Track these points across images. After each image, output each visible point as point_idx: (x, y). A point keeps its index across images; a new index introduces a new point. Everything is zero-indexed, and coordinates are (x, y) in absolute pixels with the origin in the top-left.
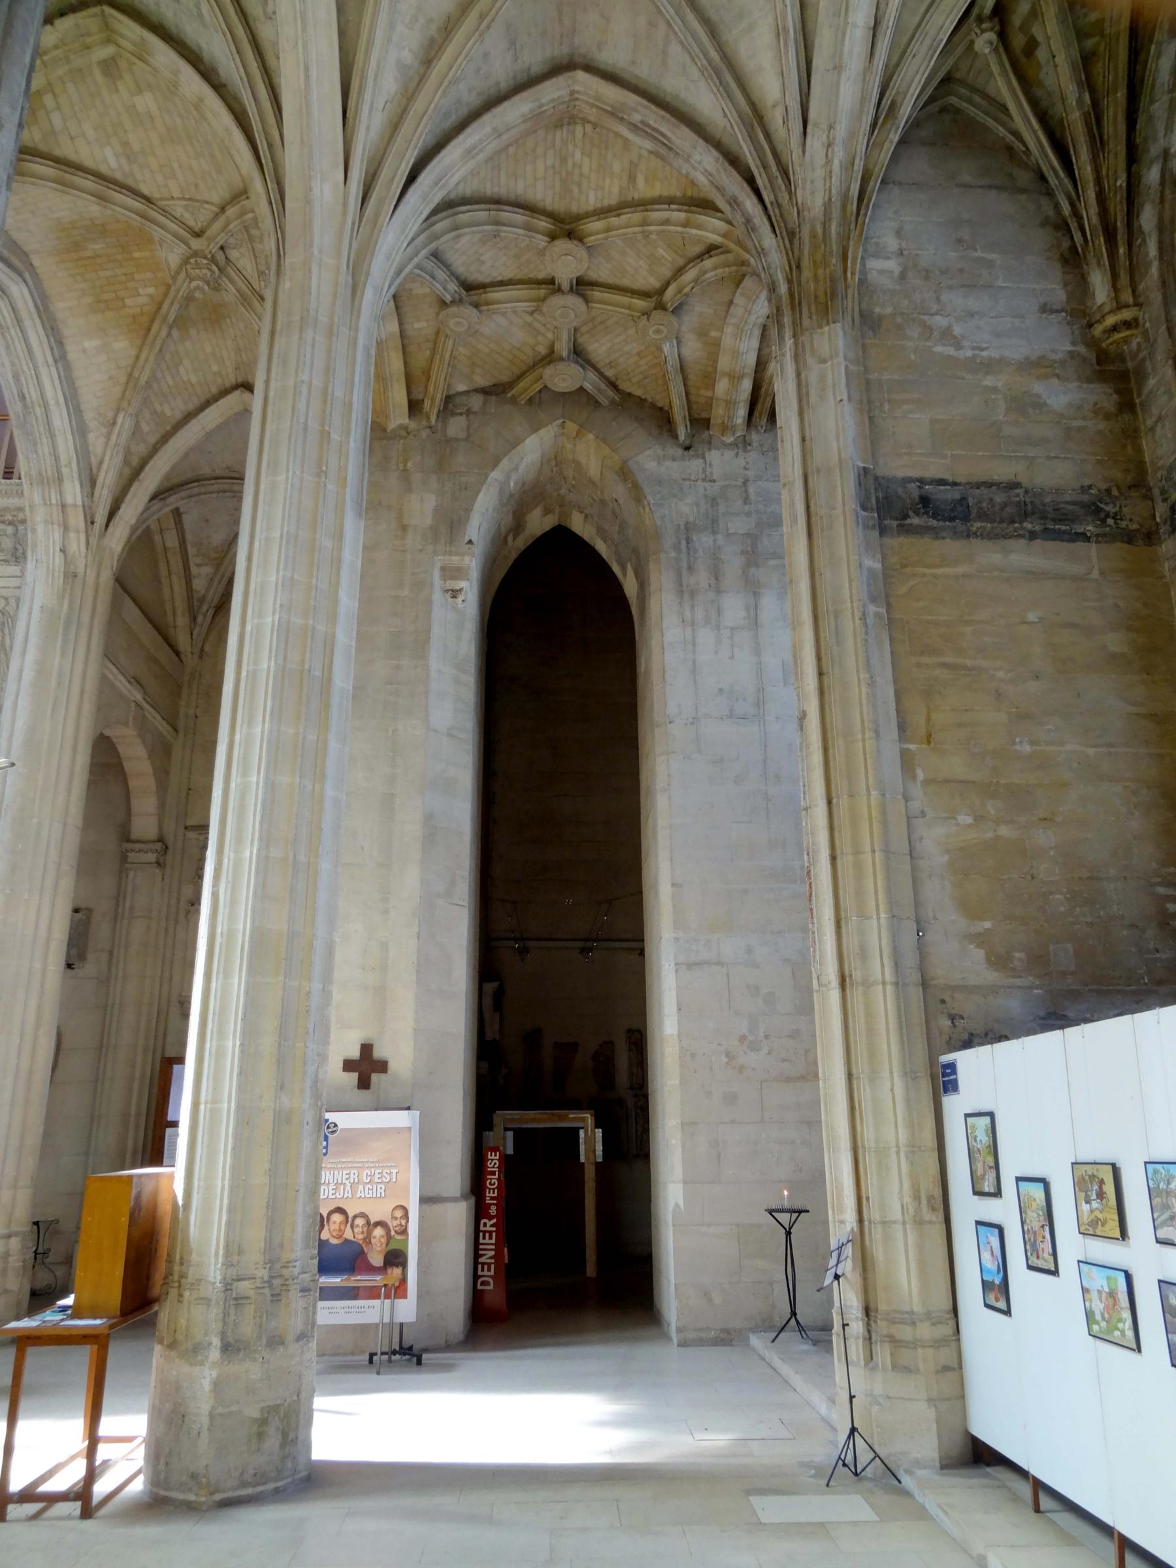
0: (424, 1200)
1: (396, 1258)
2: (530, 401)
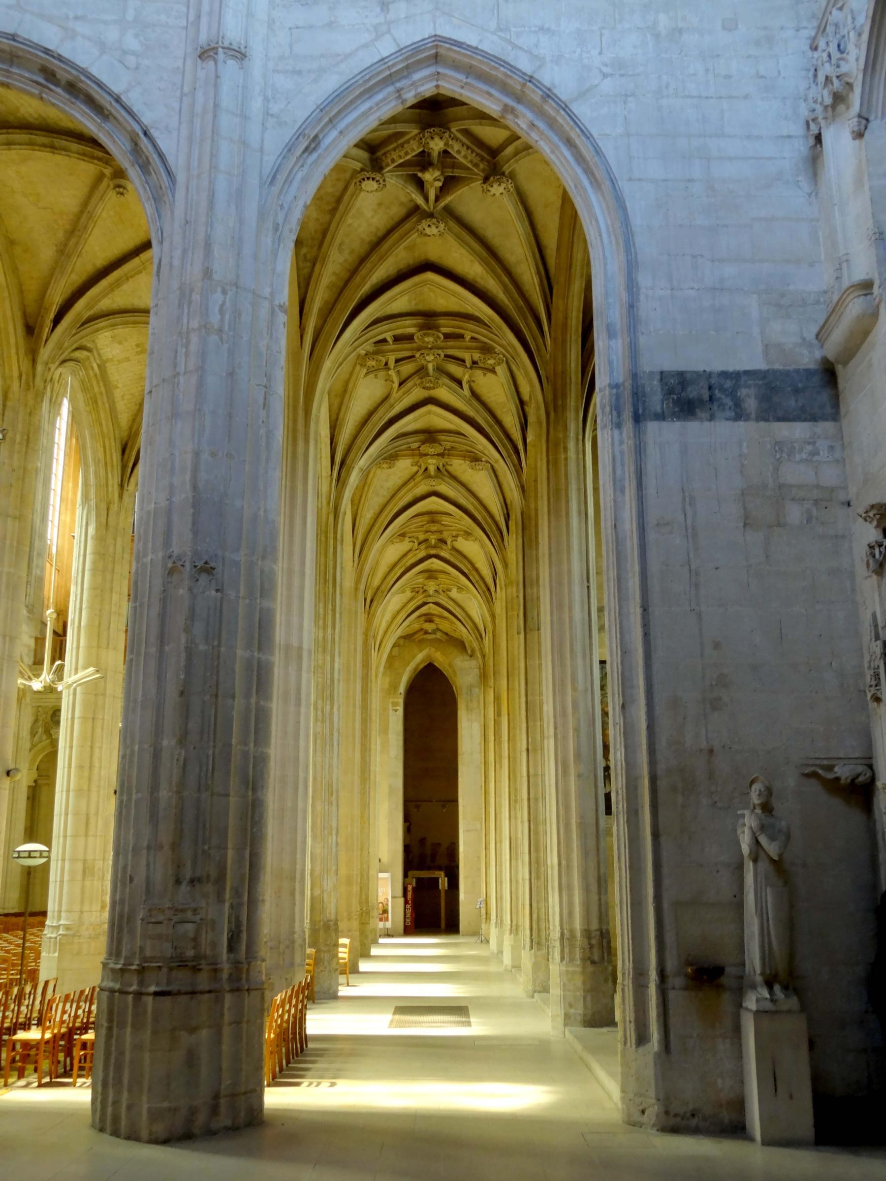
1: (385, 911)
2: (419, 641)
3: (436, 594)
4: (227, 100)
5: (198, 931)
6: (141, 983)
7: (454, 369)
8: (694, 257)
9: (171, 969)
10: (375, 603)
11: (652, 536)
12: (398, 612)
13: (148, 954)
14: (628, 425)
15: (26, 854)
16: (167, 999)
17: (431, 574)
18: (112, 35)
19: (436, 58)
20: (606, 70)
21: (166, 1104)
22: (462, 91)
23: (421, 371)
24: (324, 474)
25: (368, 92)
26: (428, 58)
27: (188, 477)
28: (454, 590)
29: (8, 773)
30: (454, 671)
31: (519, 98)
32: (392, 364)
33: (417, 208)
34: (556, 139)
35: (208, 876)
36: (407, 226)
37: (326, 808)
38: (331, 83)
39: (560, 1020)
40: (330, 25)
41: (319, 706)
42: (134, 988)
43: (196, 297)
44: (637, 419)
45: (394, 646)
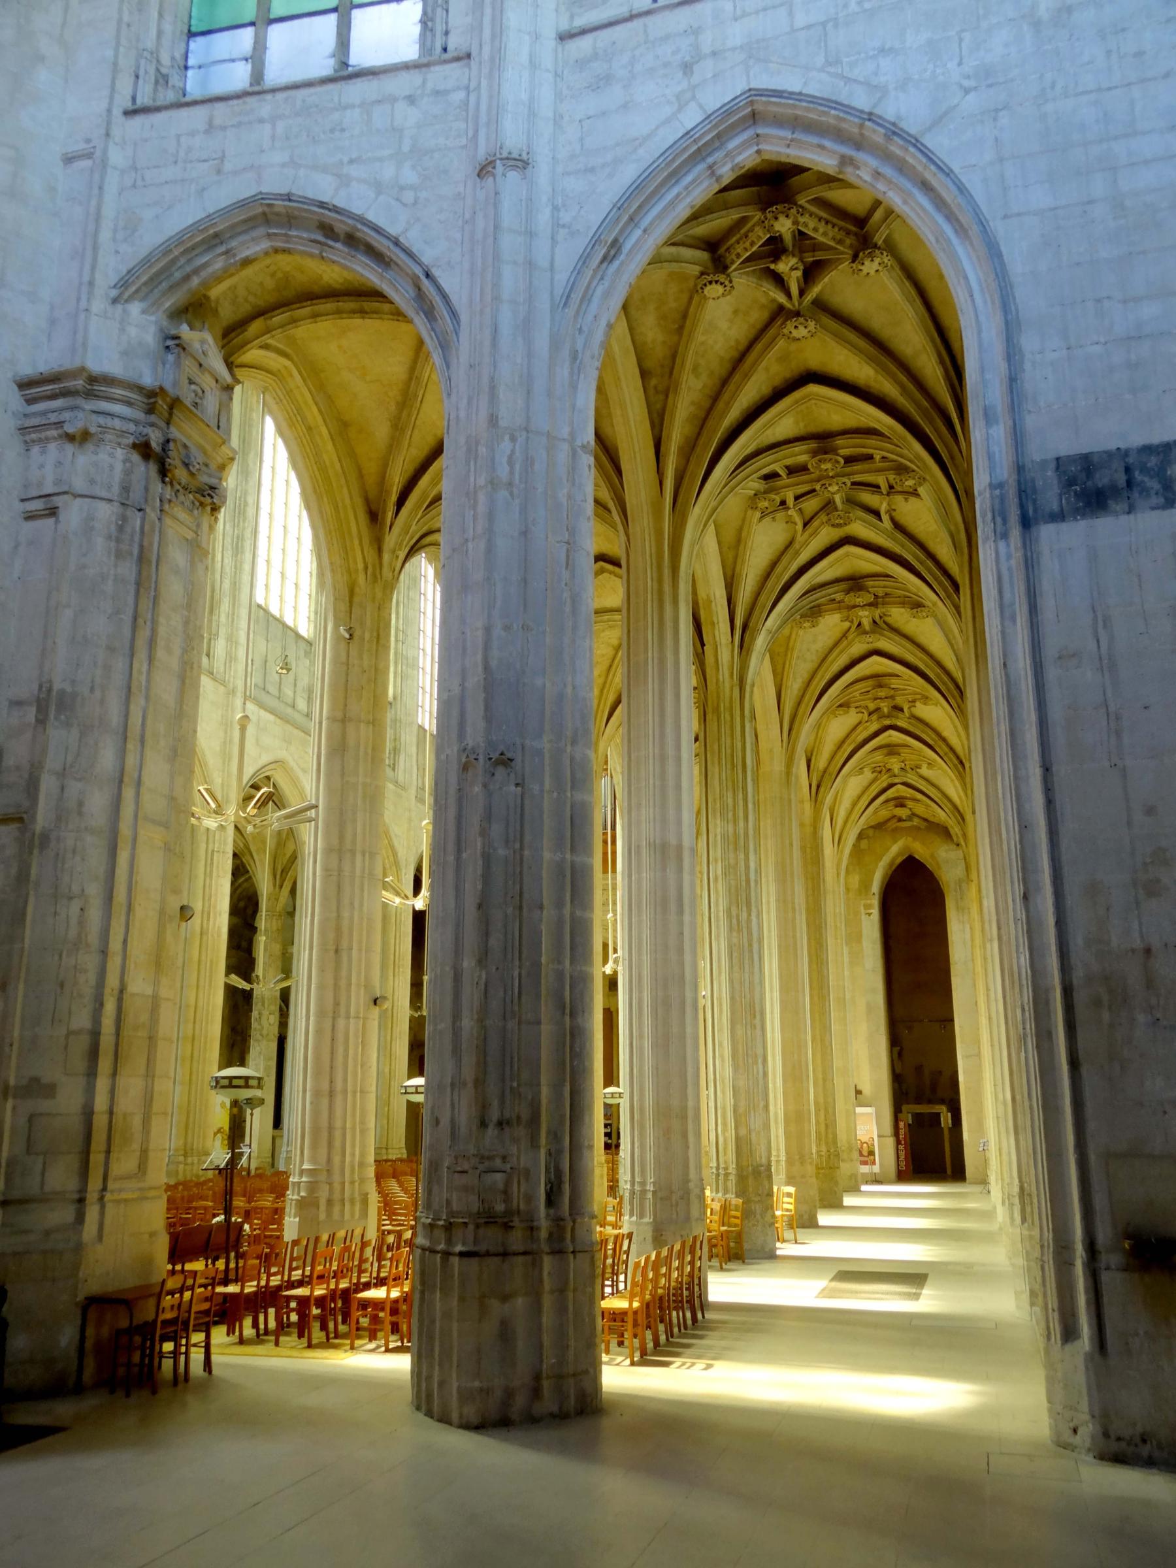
0: (879, 1136)
1: (871, 1153)
3: (902, 773)
4: (508, 217)
5: (508, 1183)
6: (449, 1241)
7: (867, 497)
8: (1098, 301)
9: (477, 1226)
10: (822, 789)
11: (1052, 673)
12: (859, 797)
13: (455, 1207)
14: (1016, 532)
15: (413, 1090)
16: (474, 1262)
17: (891, 749)
18: (388, 172)
19: (754, 117)
20: (966, 83)
21: (477, 1384)
22: (788, 151)
23: (828, 506)
24: (724, 641)
25: (674, 175)
26: (743, 119)
27: (479, 657)
28: (924, 766)
29: (375, 1002)
30: (938, 864)
31: (859, 144)
32: (790, 502)
33: (781, 308)
34: (908, 185)
35: (519, 1118)
36: (772, 332)
37: (749, 1033)
38: (629, 173)
39: (1026, 1297)
40: (625, 106)
41: (734, 913)
42: (441, 1247)
43: (482, 450)
44: (1026, 523)
45: (860, 836)
